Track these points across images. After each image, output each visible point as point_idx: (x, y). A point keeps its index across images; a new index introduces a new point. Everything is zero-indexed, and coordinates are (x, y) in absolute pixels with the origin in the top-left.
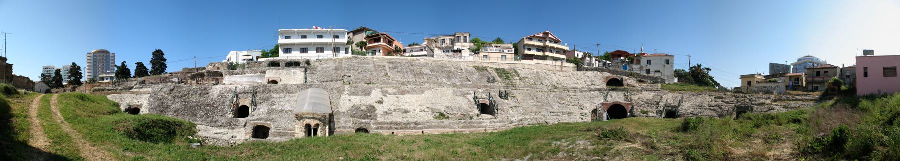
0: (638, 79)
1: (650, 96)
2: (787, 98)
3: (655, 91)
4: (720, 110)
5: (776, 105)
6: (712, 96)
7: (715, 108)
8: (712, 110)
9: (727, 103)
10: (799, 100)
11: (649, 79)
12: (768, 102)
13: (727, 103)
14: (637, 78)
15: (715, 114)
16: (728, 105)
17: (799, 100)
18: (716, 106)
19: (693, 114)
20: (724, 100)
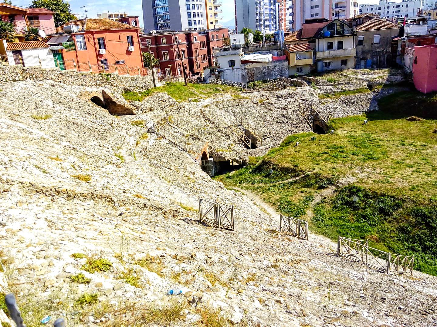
4: (289, 121)
19: (270, 133)
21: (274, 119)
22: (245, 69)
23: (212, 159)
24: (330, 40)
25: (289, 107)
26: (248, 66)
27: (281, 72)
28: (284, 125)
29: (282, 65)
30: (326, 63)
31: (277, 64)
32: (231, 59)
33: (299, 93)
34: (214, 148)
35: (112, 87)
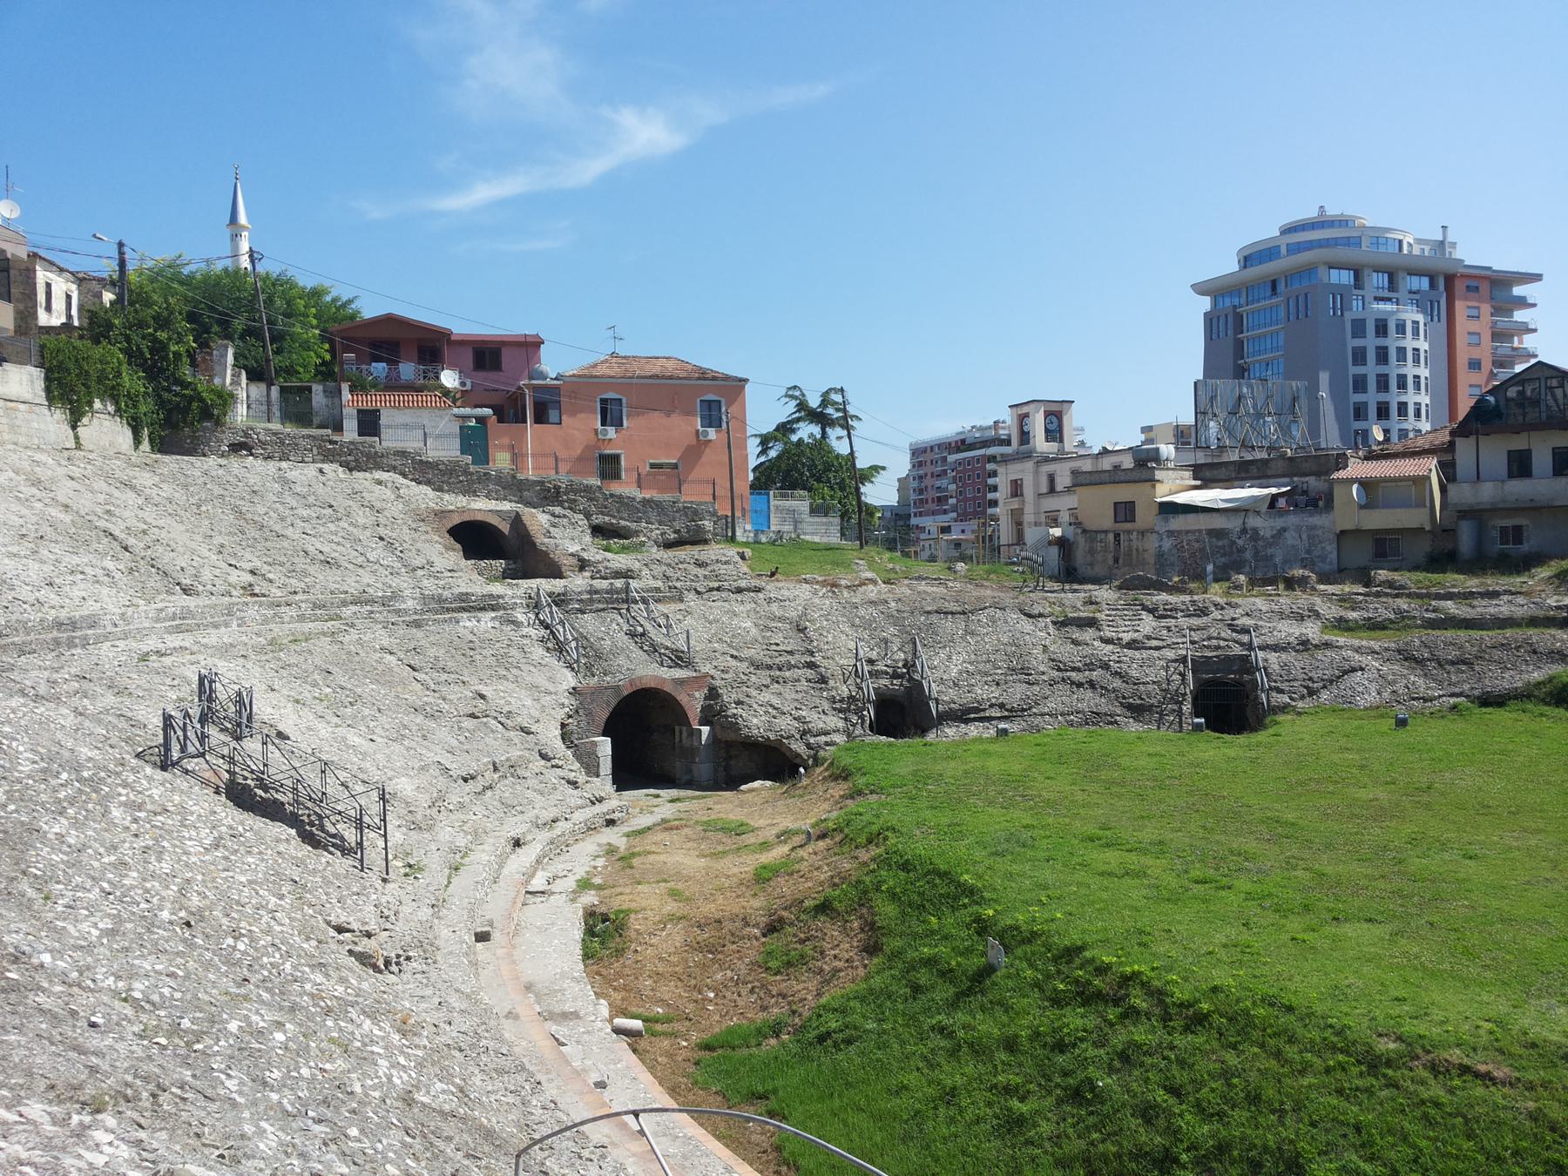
0: (599, 519)
1: (742, 619)
2: (1398, 611)
3: (739, 590)
4: (1117, 683)
5: (1357, 650)
6: (1041, 615)
7: (1096, 675)
8: (1080, 685)
9: (1133, 645)
10: (1467, 624)
11: (653, 516)
12: (1312, 630)
13: (1133, 645)
14: (588, 516)
15: (1103, 704)
16: (1145, 654)
17: (1467, 624)
18: (1090, 667)
20: (1108, 633)
21: (1059, 670)
22: (1171, 533)
23: (705, 730)
24: (1518, 443)
25: (1154, 643)
26: (1178, 523)
27: (1308, 552)
28: (1089, 694)
29: (1313, 528)
30: (1504, 530)
31: (1292, 520)
32: (1124, 493)
33: (1236, 606)
34: (728, 696)
35: (567, 512)
